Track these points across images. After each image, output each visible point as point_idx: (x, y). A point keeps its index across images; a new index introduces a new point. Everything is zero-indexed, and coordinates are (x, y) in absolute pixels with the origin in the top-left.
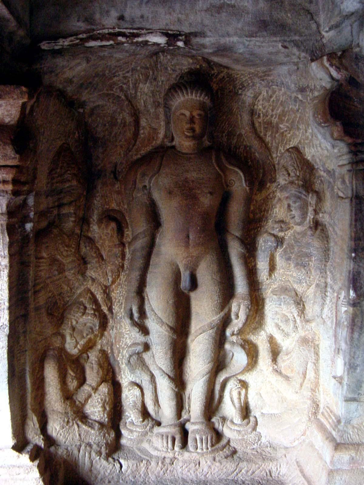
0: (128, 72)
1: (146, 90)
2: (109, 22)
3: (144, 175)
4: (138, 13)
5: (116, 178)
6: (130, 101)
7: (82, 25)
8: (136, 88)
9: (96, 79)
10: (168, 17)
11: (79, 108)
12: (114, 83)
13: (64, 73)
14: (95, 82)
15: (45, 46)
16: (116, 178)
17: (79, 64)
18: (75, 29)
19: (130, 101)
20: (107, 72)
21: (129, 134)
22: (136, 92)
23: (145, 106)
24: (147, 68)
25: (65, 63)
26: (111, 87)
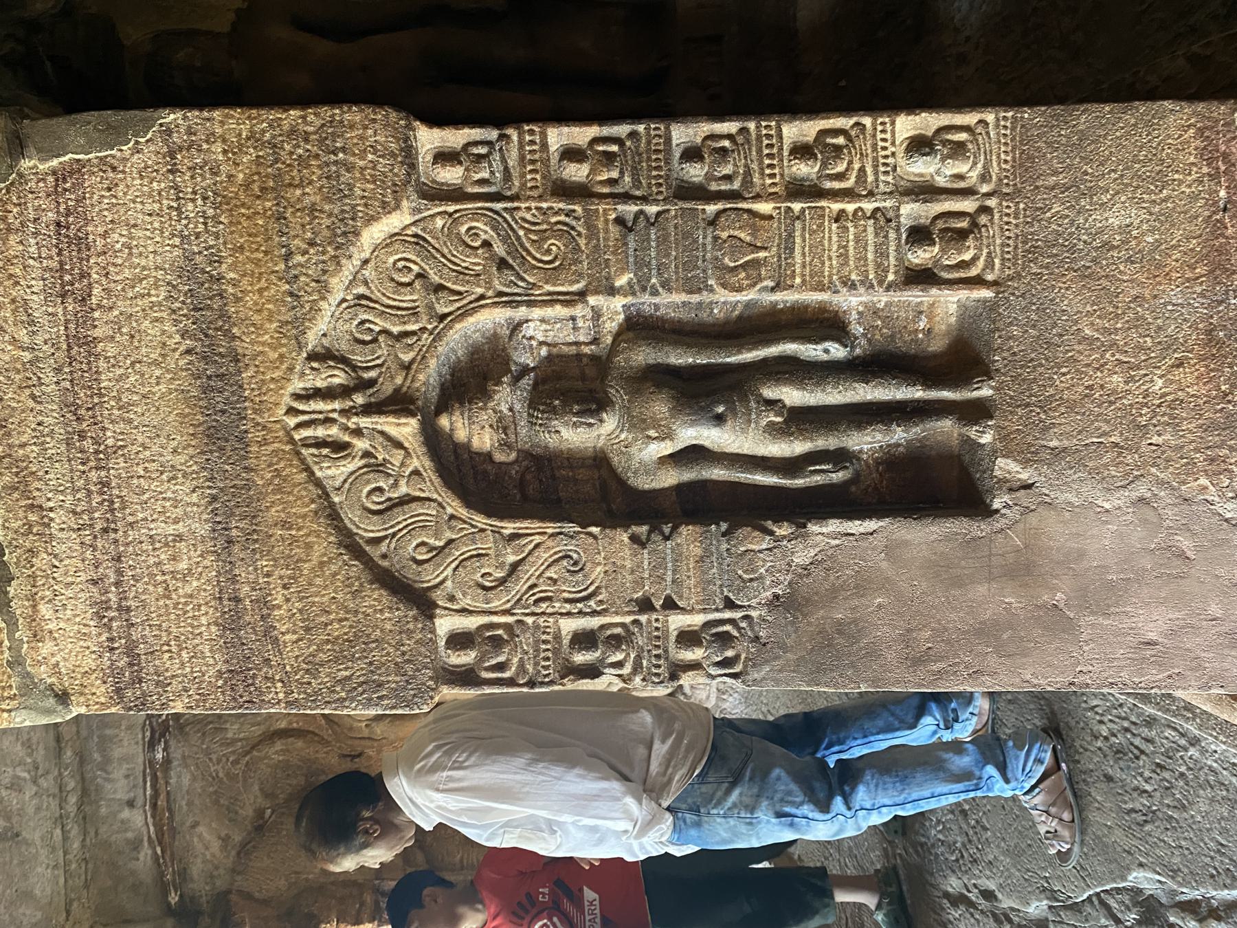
0: (210, 759)
1: (236, 727)
2: (138, 820)
3: (351, 729)
4: (123, 782)
5: (360, 755)
6: (253, 748)
7: (145, 853)
8: (234, 741)
9: (222, 801)
10: (125, 743)
11: (263, 818)
12: (227, 774)
13: (213, 855)
14: (226, 803)
15: (174, 898)
16: (360, 755)
17: (200, 836)
18: (149, 862)
19: (253, 748)
20: (211, 789)
21: (300, 744)
22: (241, 740)
23: (259, 724)
24: (204, 734)
25: (199, 860)
26: (232, 777)
